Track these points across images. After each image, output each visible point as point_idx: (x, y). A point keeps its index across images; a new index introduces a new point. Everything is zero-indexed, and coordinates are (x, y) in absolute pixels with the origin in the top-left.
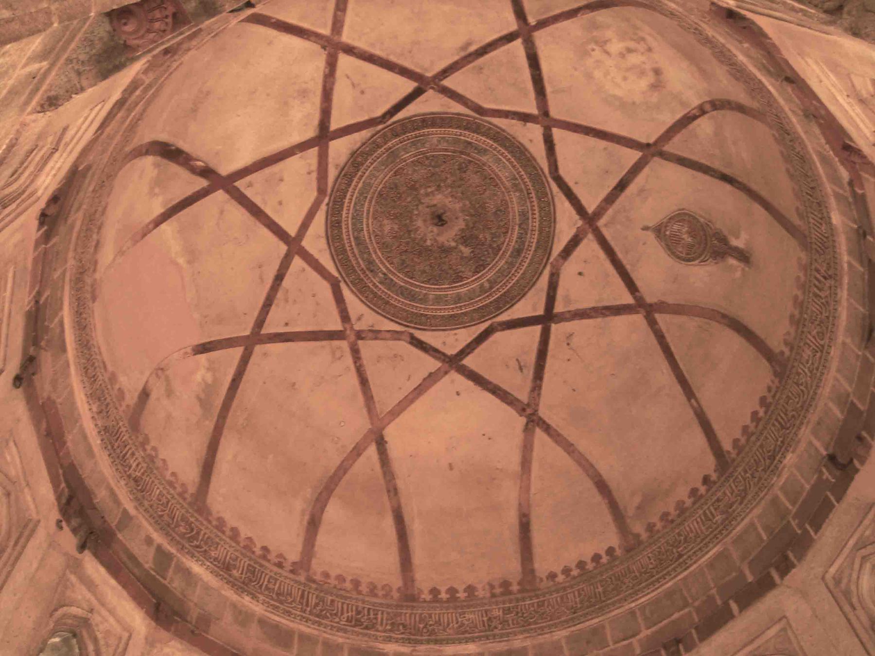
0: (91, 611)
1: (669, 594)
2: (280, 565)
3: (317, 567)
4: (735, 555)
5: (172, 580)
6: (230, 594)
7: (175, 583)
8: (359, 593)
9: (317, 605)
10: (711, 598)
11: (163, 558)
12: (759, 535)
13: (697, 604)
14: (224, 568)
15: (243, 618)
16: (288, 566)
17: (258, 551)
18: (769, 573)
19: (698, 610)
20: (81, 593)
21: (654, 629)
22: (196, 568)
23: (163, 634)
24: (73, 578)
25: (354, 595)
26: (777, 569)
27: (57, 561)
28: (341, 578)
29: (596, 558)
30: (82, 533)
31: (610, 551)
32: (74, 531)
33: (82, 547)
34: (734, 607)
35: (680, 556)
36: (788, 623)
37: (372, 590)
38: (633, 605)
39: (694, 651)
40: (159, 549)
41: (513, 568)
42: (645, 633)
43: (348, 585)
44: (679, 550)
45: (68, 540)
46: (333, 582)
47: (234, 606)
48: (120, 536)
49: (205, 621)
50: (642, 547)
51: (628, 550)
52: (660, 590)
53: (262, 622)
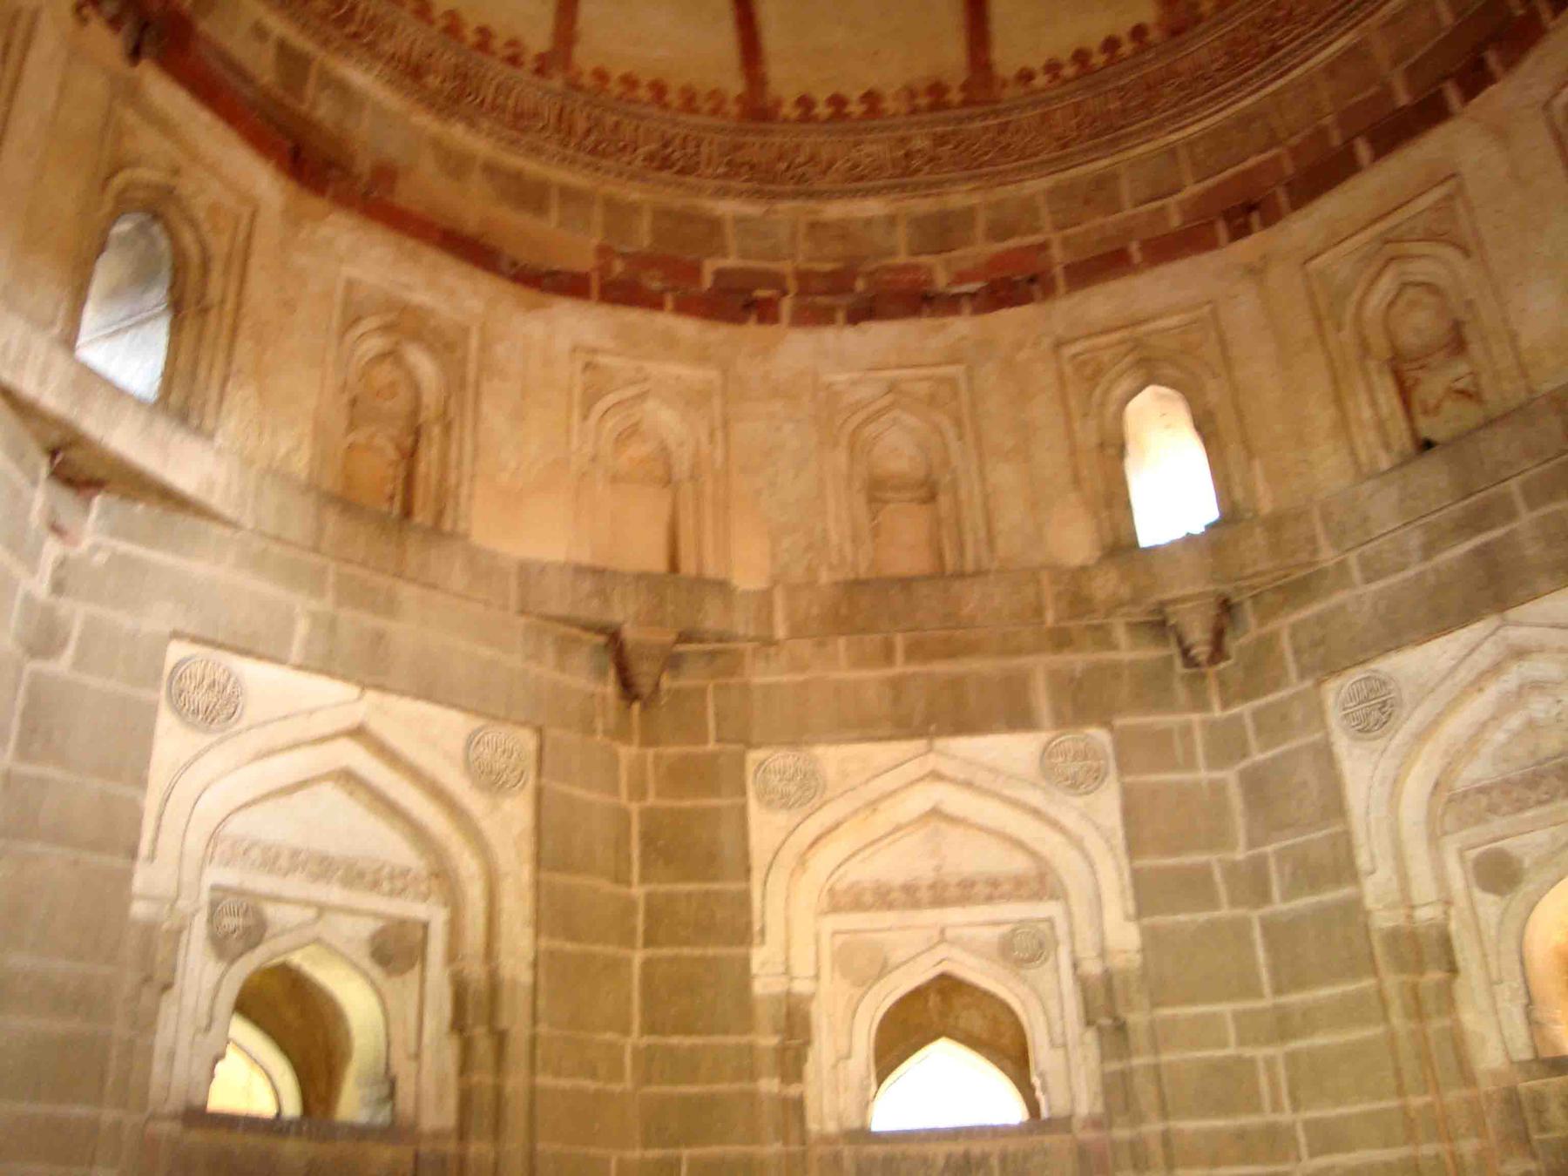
0: (176, 172)
1: (1245, 121)
2: (514, 60)
3: (585, 57)
4: (1381, 51)
5: (314, 105)
6: (425, 121)
7: (324, 110)
8: (666, 106)
9: (588, 132)
10: (1322, 133)
11: (292, 63)
12: (1435, 18)
13: (1294, 141)
14: (411, 72)
15: (456, 164)
16: (529, 63)
17: (471, 37)
18: (1440, 91)
19: (1295, 152)
20: (148, 141)
21: (1210, 183)
22: (360, 77)
23: (316, 204)
24: (130, 117)
25: (655, 111)
26: (1461, 84)
27: (93, 85)
28: (630, 82)
29: (1111, 44)
30: (128, 26)
31: (1138, 32)
32: (114, 23)
33: (135, 54)
34: (1363, 150)
35: (1274, 49)
36: (1460, 188)
37: (689, 101)
38: (1174, 137)
39: (1280, 225)
40: (283, 47)
41: (951, 57)
42: (1192, 190)
43: (643, 93)
44: (1274, 36)
45: (107, 44)
46: (615, 88)
47: (436, 143)
48: (204, 26)
49: (386, 174)
50: (1203, 26)
51: (1175, 32)
52: (1230, 111)
53: (491, 170)
